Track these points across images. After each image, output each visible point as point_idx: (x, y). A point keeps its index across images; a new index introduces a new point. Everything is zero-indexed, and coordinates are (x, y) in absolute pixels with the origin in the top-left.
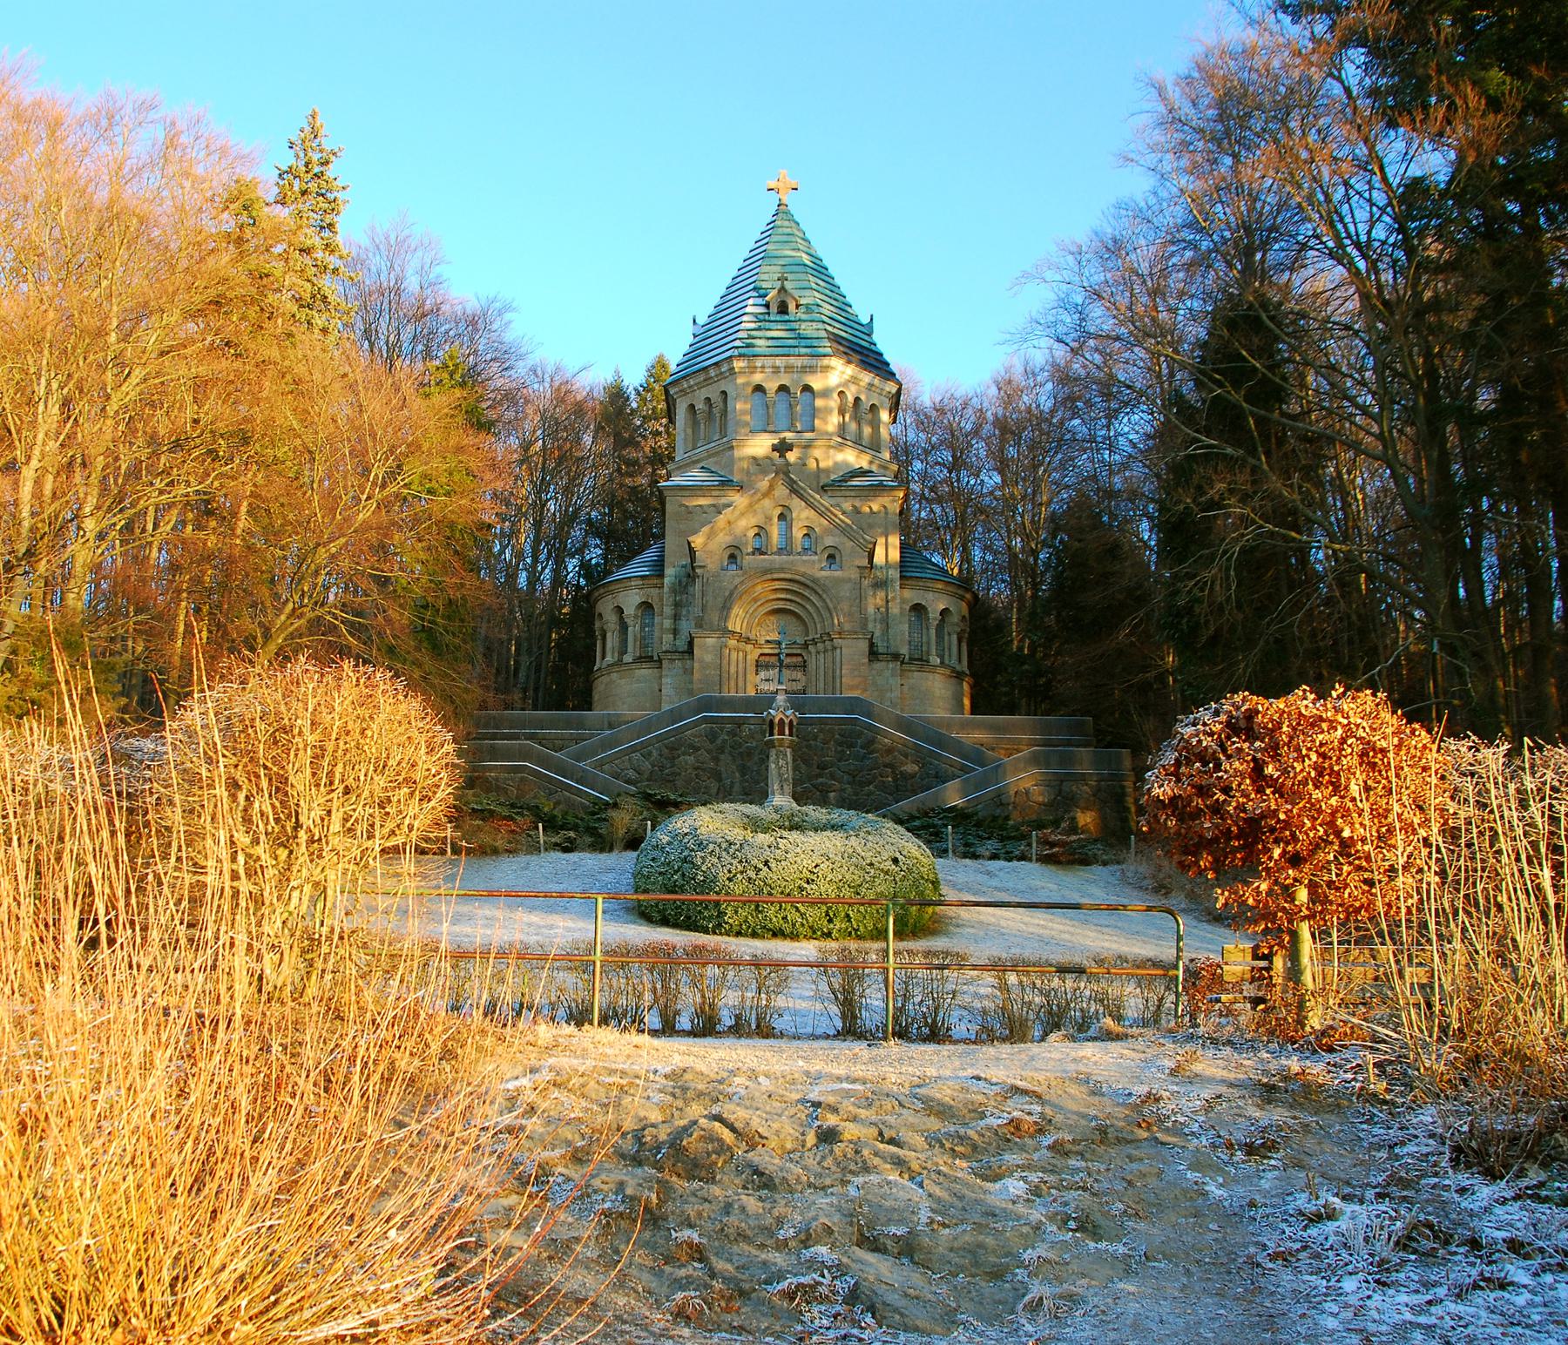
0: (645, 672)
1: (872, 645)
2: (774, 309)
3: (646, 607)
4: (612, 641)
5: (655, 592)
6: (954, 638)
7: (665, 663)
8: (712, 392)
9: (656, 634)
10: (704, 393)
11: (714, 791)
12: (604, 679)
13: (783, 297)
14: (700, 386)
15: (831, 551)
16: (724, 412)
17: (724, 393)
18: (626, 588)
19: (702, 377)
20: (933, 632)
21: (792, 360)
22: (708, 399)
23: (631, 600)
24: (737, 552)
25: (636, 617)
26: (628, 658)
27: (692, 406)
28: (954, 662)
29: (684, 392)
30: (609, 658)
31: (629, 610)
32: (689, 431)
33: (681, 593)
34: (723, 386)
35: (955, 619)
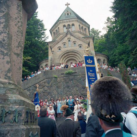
8: (57, 29)
13: (68, 13)
14: (55, 28)
15: (80, 45)
17: (59, 28)
19: (55, 27)
21: (70, 20)
24: (60, 48)
29: (53, 31)
34: (58, 27)
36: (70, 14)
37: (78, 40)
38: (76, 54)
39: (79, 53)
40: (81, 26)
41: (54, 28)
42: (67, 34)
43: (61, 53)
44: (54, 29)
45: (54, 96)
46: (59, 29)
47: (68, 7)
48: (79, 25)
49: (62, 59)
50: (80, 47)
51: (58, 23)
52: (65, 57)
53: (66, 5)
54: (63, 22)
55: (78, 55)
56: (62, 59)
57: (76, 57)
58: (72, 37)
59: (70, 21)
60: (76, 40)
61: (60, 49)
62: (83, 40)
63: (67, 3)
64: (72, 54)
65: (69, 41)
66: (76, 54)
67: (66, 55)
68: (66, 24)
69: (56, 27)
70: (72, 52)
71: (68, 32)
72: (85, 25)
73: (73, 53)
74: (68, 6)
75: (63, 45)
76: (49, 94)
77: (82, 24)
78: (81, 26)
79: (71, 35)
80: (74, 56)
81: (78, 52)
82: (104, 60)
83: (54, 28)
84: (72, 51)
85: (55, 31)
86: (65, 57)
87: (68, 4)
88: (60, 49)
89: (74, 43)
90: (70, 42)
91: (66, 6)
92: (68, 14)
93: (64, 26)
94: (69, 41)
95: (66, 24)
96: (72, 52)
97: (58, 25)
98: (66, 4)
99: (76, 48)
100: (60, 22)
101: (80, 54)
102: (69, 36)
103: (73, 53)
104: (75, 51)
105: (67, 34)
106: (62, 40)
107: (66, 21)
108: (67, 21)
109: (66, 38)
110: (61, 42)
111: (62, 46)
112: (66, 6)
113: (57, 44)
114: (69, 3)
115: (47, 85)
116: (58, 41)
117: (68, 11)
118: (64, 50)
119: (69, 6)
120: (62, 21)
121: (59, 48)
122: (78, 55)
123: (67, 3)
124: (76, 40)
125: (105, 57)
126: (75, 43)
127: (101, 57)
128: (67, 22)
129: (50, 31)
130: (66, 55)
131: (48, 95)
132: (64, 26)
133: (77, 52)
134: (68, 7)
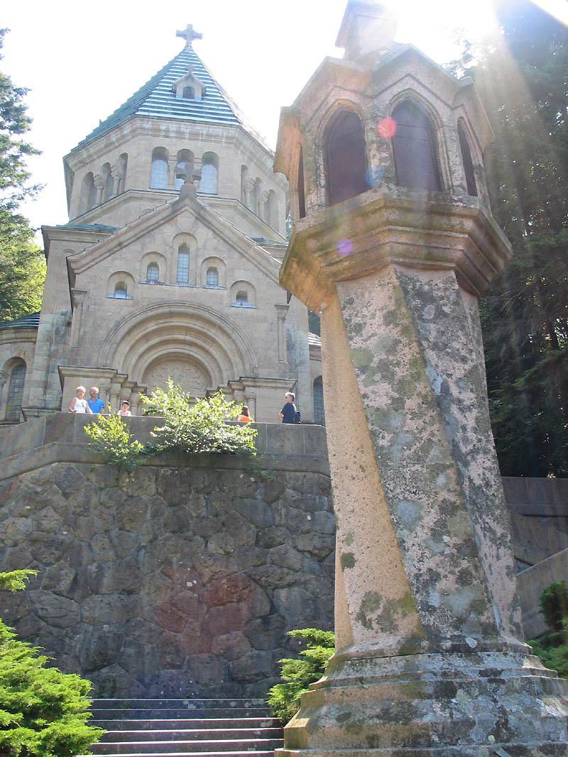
2: (180, 92)
5: (27, 346)
10: (103, 160)
11: (64, 585)
13: (189, 84)
14: (100, 154)
15: (243, 288)
17: (124, 156)
19: (102, 143)
21: (198, 128)
22: (107, 165)
24: (128, 281)
27: (90, 176)
29: (83, 163)
32: (85, 200)
33: (57, 343)
34: (123, 150)
36: (204, 95)
37: (237, 255)
38: (212, 332)
39: (229, 332)
41: (92, 151)
42: (175, 210)
43: (125, 311)
45: (93, 568)
46: (125, 166)
47: (187, 54)
48: (244, 168)
49: (125, 348)
50: (242, 297)
51: (127, 129)
52: (146, 337)
53: (179, 34)
54: (156, 132)
55: (221, 339)
56: (125, 348)
57: (207, 351)
58: (203, 233)
59: (195, 136)
60: (223, 252)
61: (121, 288)
62: (264, 262)
63: (190, 26)
64: (188, 330)
65: (183, 249)
66: (212, 332)
67: (152, 326)
68: (173, 148)
69: (109, 147)
70: (192, 316)
71: (187, 201)
73: (197, 325)
75: (145, 269)
76: (64, 552)
80: (200, 342)
81: (223, 325)
83: (92, 151)
84: (190, 311)
85: (97, 171)
86: (146, 337)
87: (189, 35)
88: (121, 288)
90: (184, 258)
91: (181, 43)
92: (188, 93)
93: (159, 154)
95: (173, 148)
96: (192, 316)
97: (123, 140)
98: (183, 28)
99: (219, 298)
100: (138, 123)
101: (234, 336)
102: (185, 220)
103: (197, 325)
104: (207, 315)
106: (147, 240)
107: (173, 127)
108: (178, 132)
109: (169, 231)
110: (136, 247)
111: (139, 269)
112: (181, 43)
113: (111, 252)
114: (196, 29)
115: (58, 499)
116: (122, 239)
117: (190, 77)
118: (146, 293)
120: (148, 125)
121: (117, 279)
122: (221, 339)
123: (190, 26)
124: (224, 255)
129: (66, 160)
130: (152, 326)
131: (58, 560)
132: (159, 154)
133: (218, 322)
134: (187, 54)
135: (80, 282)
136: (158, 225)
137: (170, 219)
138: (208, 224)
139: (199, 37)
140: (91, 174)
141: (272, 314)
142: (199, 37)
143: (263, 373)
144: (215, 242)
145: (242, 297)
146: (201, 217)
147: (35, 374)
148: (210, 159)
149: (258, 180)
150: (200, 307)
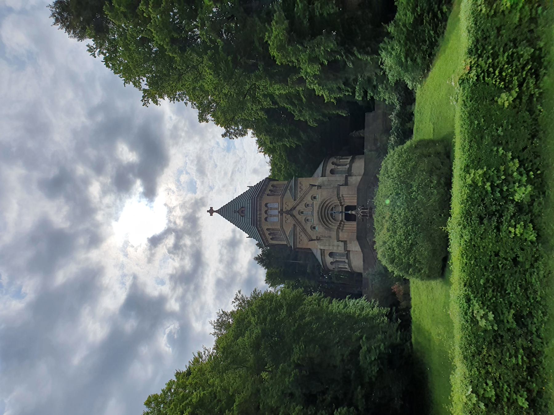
0: (351, 255)
1: (342, 185)
3: (331, 254)
4: (341, 266)
6: (341, 160)
7: (348, 249)
8: (267, 233)
9: (338, 252)
10: (267, 235)
12: (353, 268)
16: (273, 230)
17: (267, 229)
18: (325, 261)
20: (339, 167)
21: (258, 209)
23: (329, 260)
25: (334, 258)
26: (347, 261)
28: (349, 160)
29: (267, 241)
30: (347, 267)
31: (331, 260)
34: (265, 229)
35: (335, 160)
38: (325, 205)
40: (268, 192)
42: (292, 216)
44: (266, 238)
48: (268, 195)
50: (315, 198)
52: (327, 221)
53: (211, 215)
54: (260, 221)
55: (327, 203)
58: (298, 208)
59: (260, 210)
65: (302, 213)
66: (325, 205)
68: (264, 216)
69: (264, 235)
72: (267, 186)
74: (216, 211)
77: (265, 190)
78: (268, 192)
79: (294, 208)
82: (333, 163)
86: (327, 221)
88: (314, 228)
89: (307, 205)
93: (266, 219)
94: (302, 213)
97: (262, 230)
99: (317, 203)
102: (295, 213)
105: (292, 216)
107: (258, 216)
109: (298, 217)
110: (303, 224)
112: (214, 214)
113: (305, 230)
119: (214, 209)
122: (327, 203)
125: (327, 162)
126: (308, 205)
127: (327, 168)
128: (260, 214)
132: (266, 219)
135: (314, 238)
136: (297, 220)
137: (294, 216)
138: (295, 207)
139: (211, 208)
140: (271, 239)
141: (320, 190)
142: (211, 208)
143: (336, 193)
144: (300, 205)
145: (315, 198)
146: (294, 208)
147: (335, 250)
148: (266, 205)
149: (270, 190)
150: (319, 208)
